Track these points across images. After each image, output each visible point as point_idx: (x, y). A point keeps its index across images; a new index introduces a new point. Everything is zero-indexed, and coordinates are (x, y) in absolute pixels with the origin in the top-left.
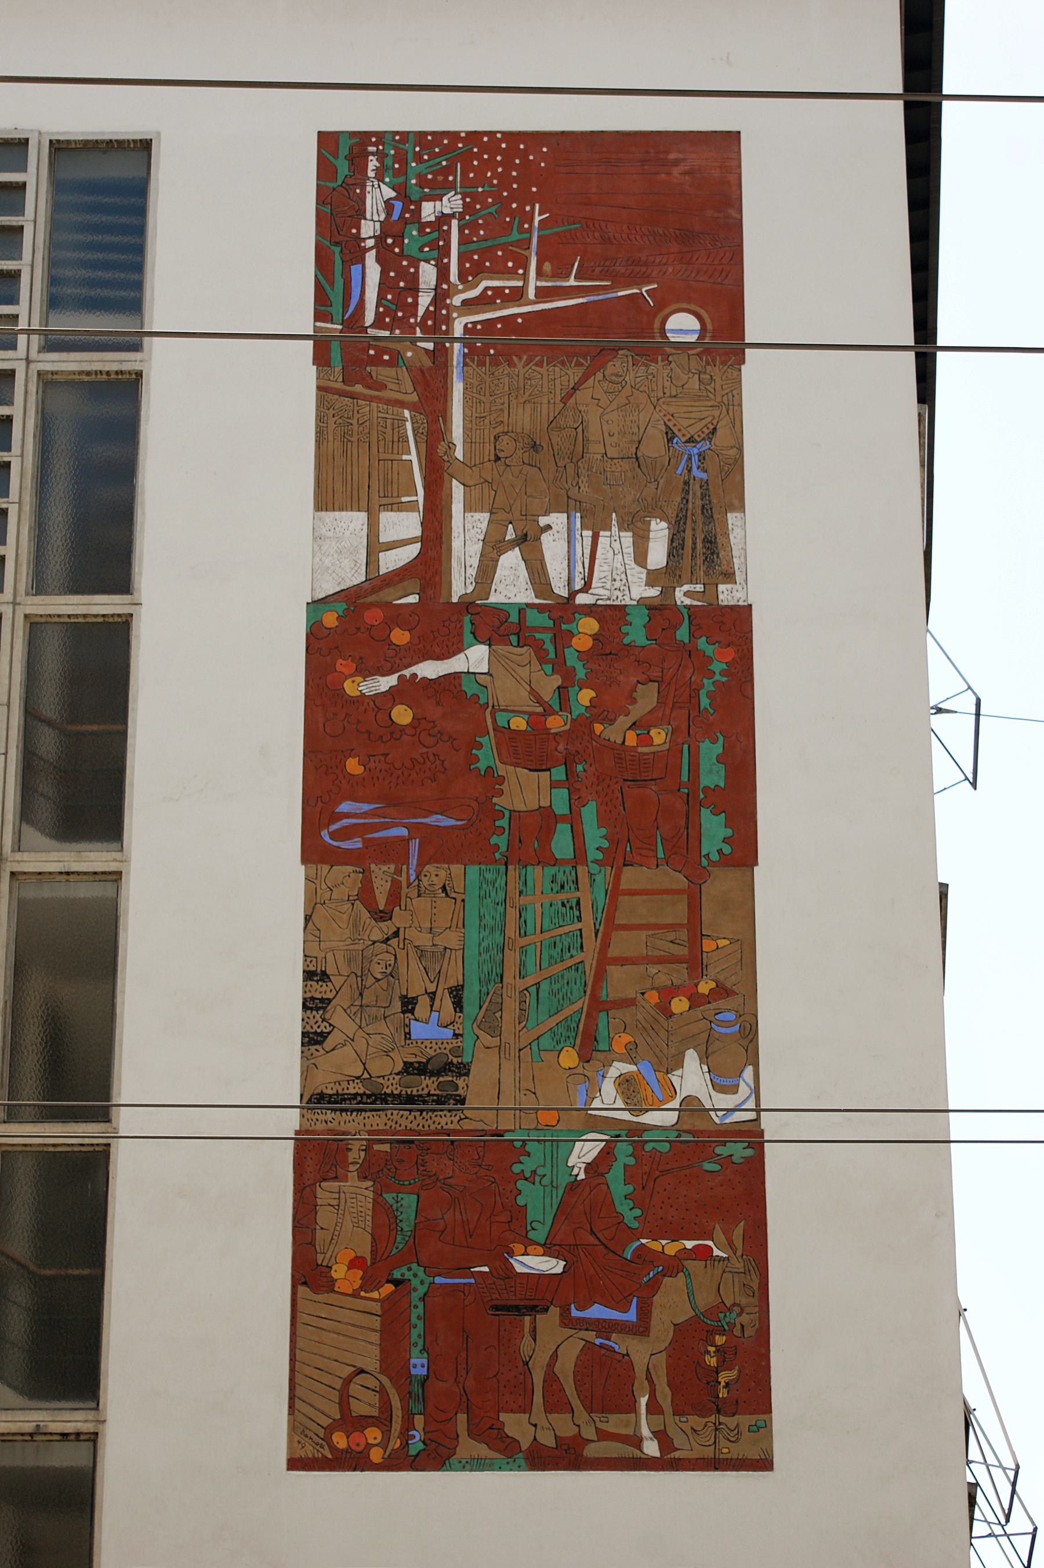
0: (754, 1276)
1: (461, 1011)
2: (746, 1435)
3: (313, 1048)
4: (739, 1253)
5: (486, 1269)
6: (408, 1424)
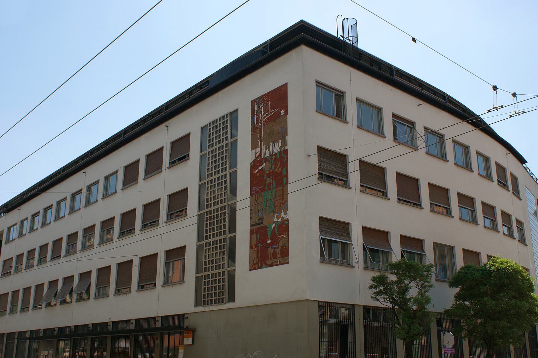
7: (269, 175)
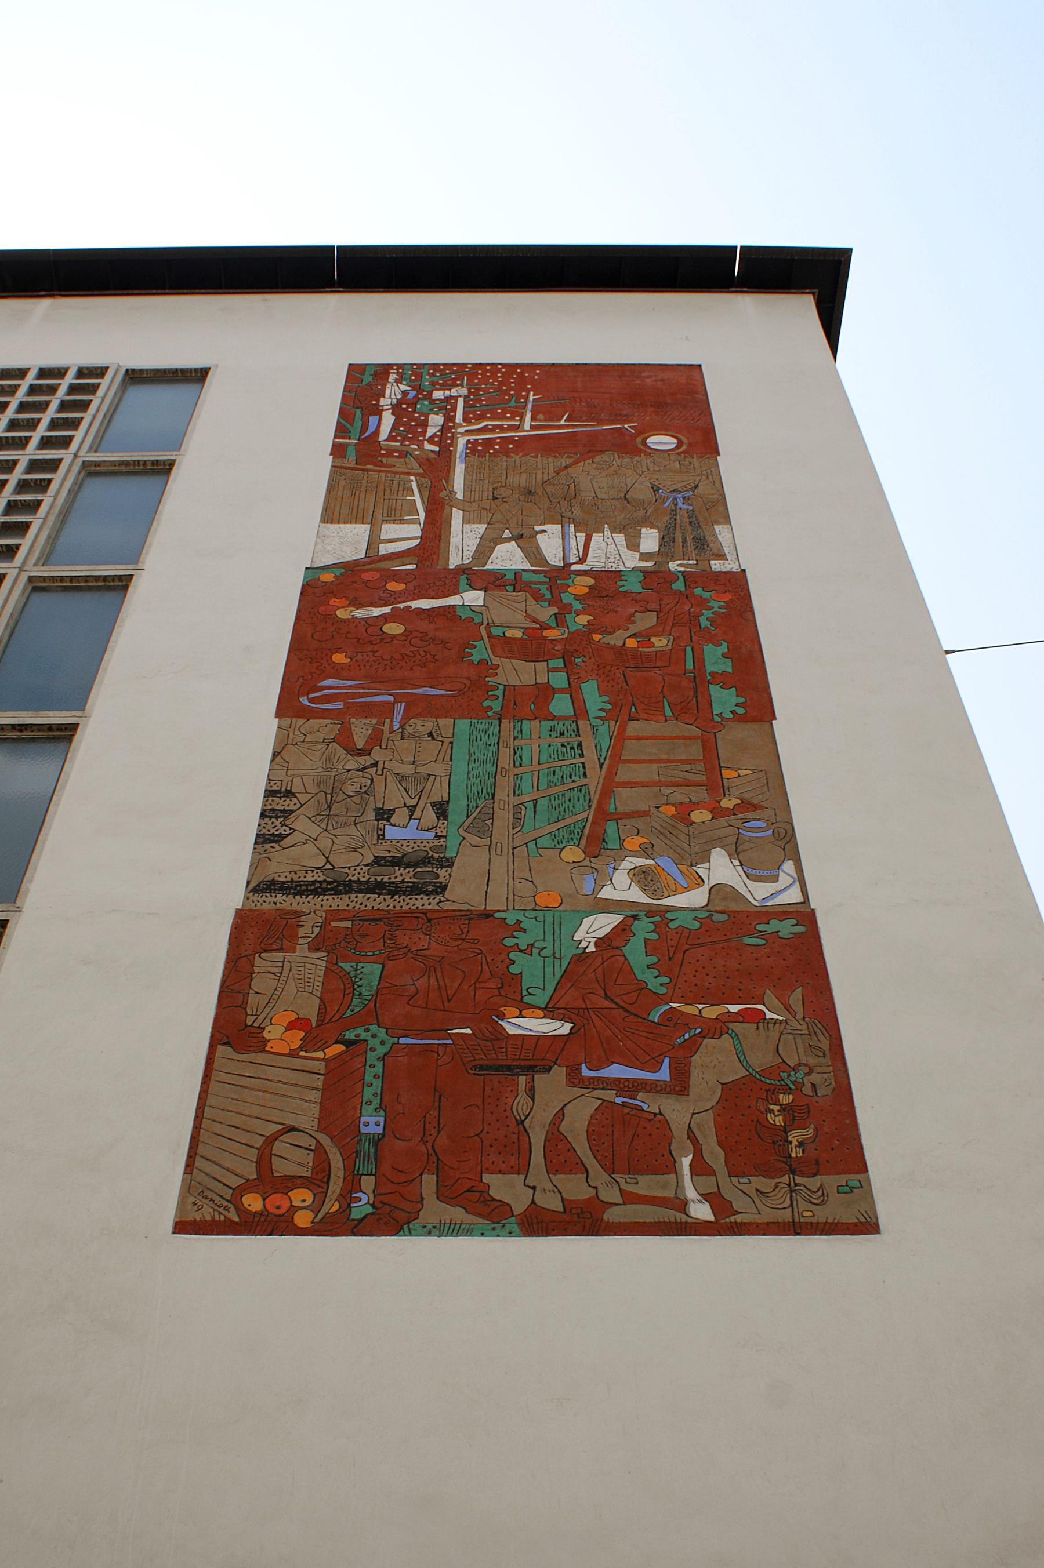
0: (821, 1037)
1: (446, 818)
2: (834, 1197)
3: (267, 846)
4: (800, 1016)
5: (468, 1031)
6: (352, 1184)
7: (531, 647)
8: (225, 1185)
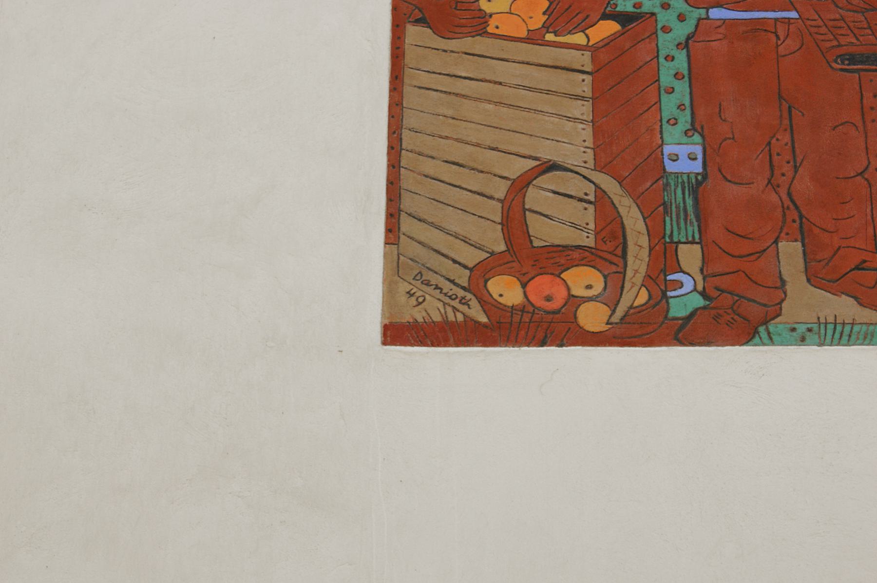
6: (664, 259)
8: (455, 261)
